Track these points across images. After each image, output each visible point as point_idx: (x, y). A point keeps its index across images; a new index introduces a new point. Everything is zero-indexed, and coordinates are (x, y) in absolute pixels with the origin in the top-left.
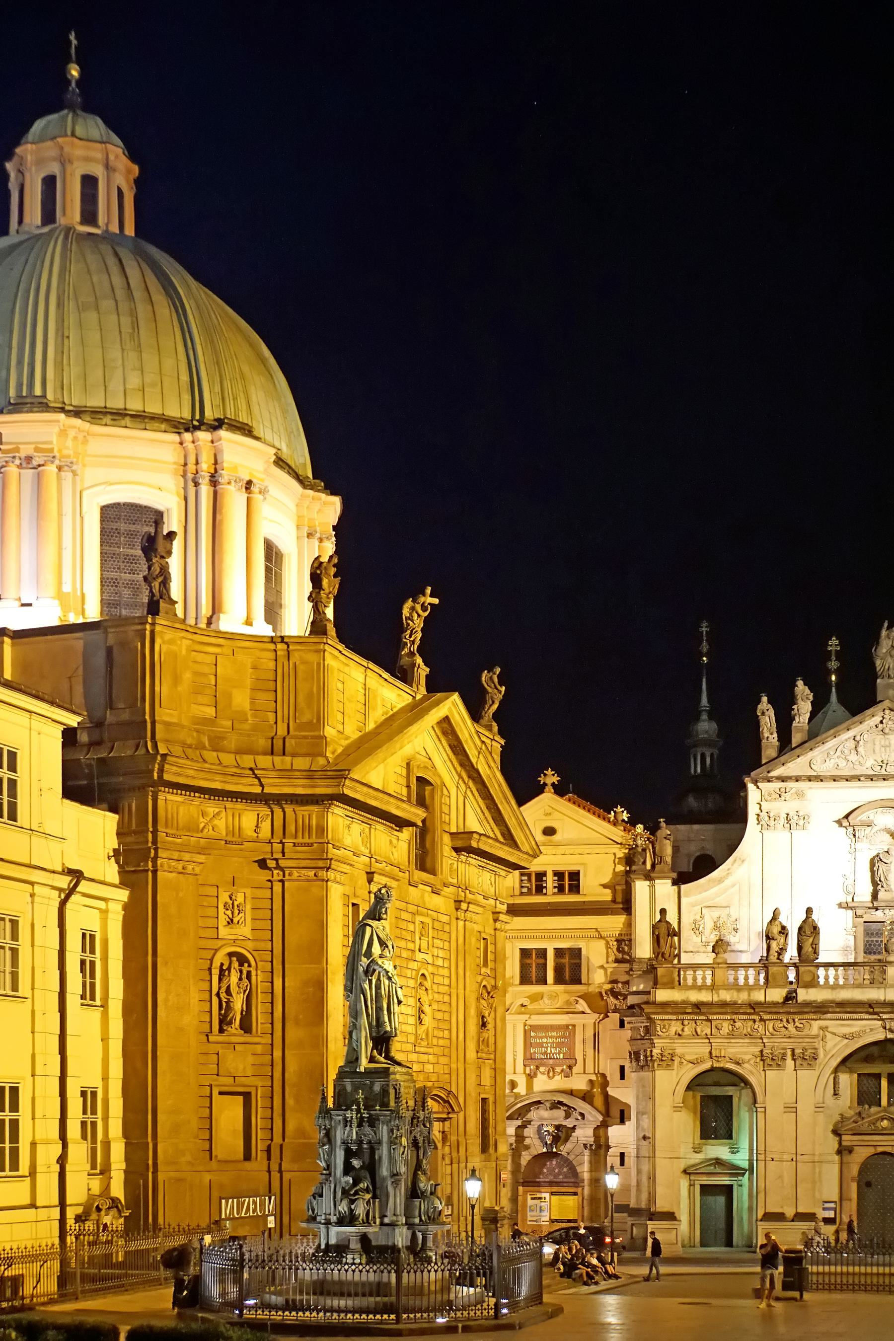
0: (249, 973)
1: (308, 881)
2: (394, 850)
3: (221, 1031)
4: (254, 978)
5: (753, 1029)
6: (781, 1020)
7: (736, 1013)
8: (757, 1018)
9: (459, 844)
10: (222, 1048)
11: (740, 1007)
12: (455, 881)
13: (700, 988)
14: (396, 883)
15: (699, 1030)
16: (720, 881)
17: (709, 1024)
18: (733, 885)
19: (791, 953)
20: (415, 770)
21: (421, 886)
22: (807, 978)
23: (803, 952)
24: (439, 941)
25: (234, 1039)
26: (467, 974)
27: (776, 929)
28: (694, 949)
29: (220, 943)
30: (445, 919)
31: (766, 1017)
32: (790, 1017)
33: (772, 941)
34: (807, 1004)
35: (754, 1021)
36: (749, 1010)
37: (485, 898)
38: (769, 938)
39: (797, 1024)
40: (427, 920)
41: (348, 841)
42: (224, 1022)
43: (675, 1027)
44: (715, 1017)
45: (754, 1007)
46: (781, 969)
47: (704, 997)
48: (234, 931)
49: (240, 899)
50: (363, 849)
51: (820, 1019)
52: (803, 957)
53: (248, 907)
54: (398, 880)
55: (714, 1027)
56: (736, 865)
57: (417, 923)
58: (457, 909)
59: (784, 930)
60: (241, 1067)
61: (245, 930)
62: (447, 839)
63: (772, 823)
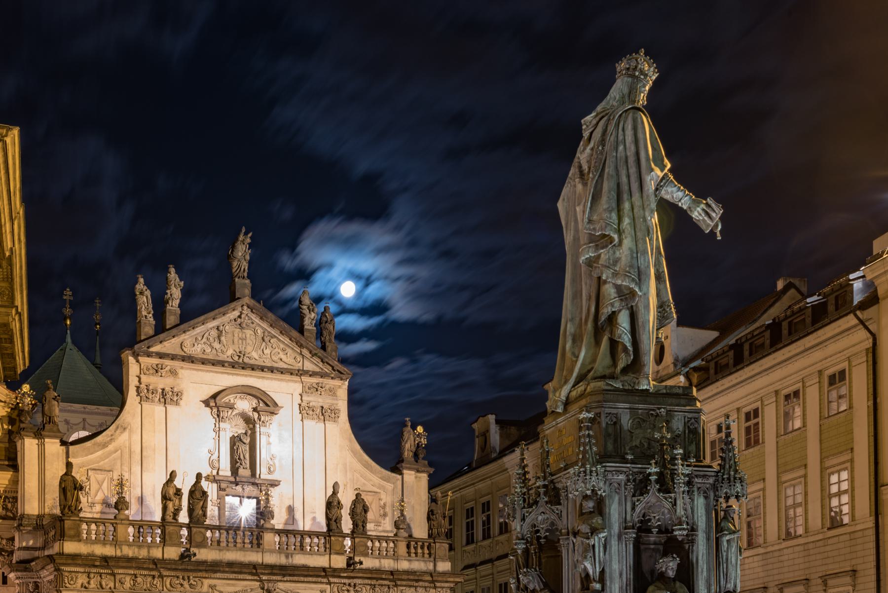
5: (152, 584)
6: (178, 577)
7: (139, 568)
8: (156, 573)
11: (144, 563)
13: (104, 543)
15: (104, 584)
16: (104, 445)
17: (113, 578)
18: (116, 451)
19: (183, 517)
22: (198, 539)
23: (195, 514)
27: (171, 491)
28: (91, 504)
31: (165, 573)
32: (186, 574)
33: (168, 502)
34: (204, 563)
35: (154, 577)
36: (151, 566)
38: (165, 498)
39: (192, 581)
43: (82, 579)
44: (121, 571)
45: (156, 563)
46: (176, 528)
47: (108, 551)
51: (211, 578)
52: (195, 519)
55: (117, 581)
56: (118, 432)
59: (178, 493)
63: (150, 396)
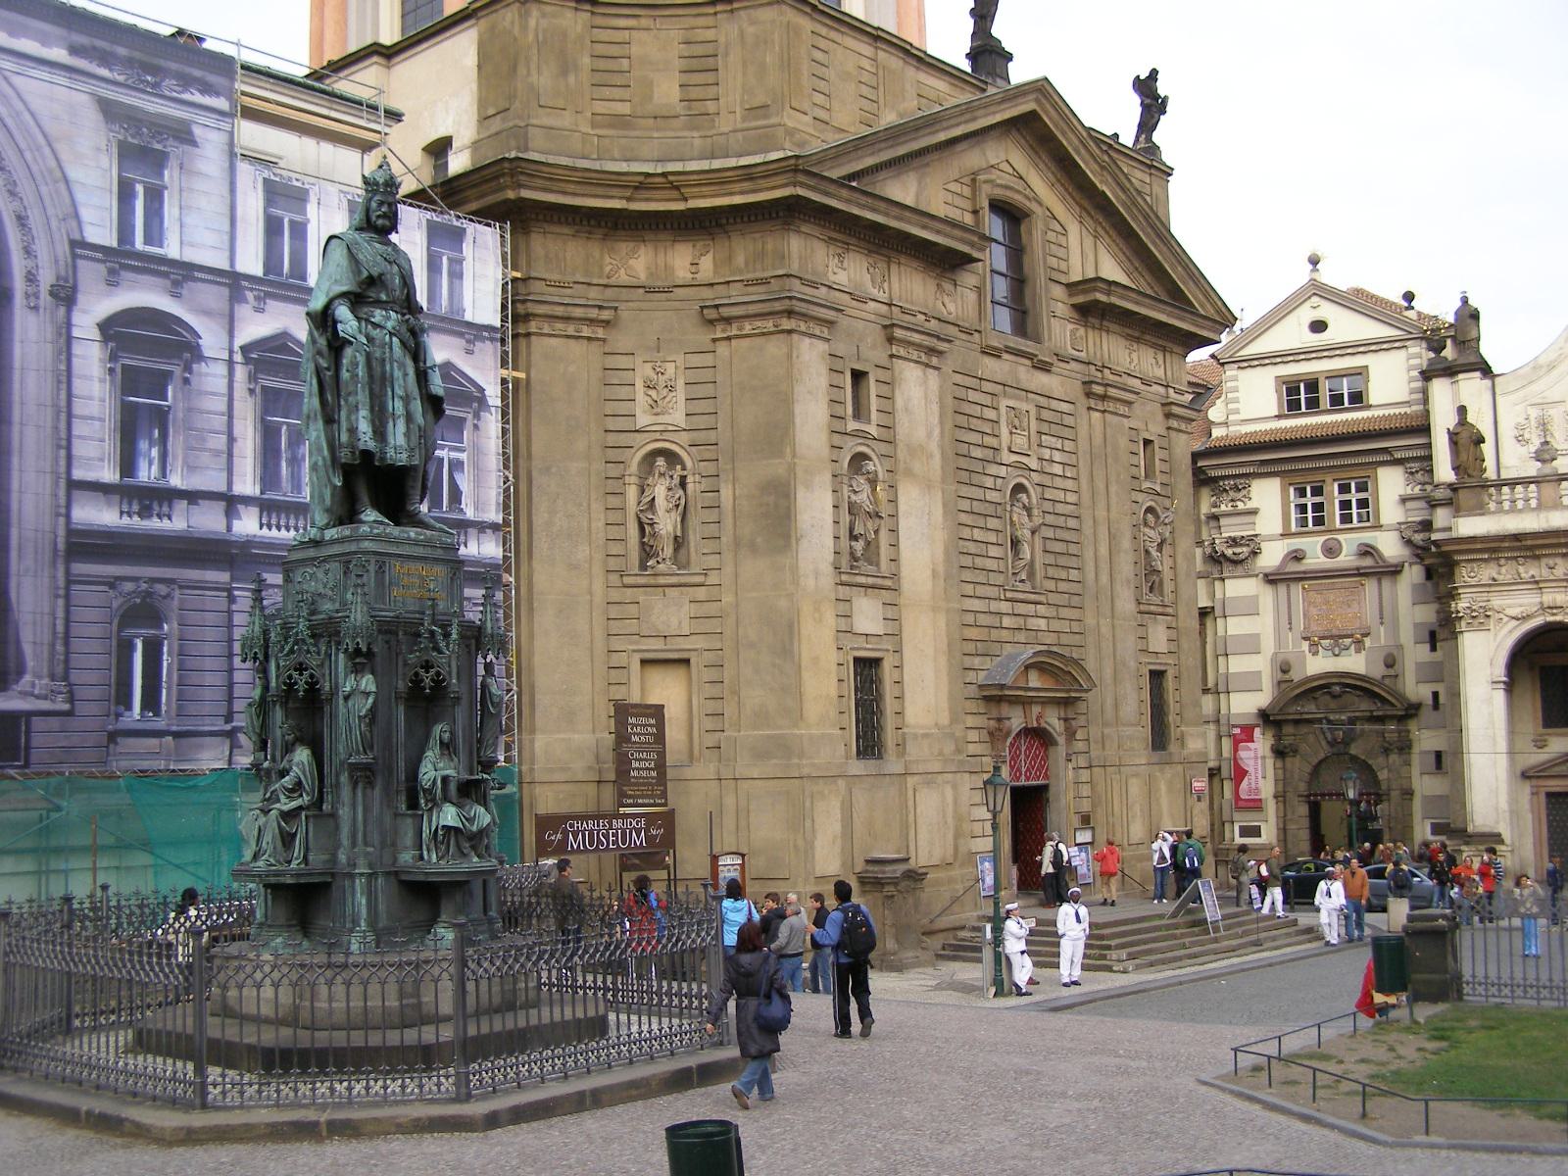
0: (683, 478)
1: (764, 334)
2: (946, 300)
3: (643, 566)
4: (690, 487)
9: (1080, 299)
10: (646, 594)
12: (1083, 355)
14: (946, 345)
20: (986, 189)
21: (1005, 356)
24: (1054, 439)
25: (662, 580)
26: (1113, 489)
29: (639, 438)
30: (1064, 407)
37: (1146, 382)
40: (1024, 406)
41: (841, 278)
42: (647, 552)
48: (661, 419)
49: (670, 369)
50: (875, 292)
53: (680, 383)
54: (950, 341)
57: (1003, 410)
58: (1089, 395)
60: (674, 621)
61: (678, 417)
62: (1058, 291)
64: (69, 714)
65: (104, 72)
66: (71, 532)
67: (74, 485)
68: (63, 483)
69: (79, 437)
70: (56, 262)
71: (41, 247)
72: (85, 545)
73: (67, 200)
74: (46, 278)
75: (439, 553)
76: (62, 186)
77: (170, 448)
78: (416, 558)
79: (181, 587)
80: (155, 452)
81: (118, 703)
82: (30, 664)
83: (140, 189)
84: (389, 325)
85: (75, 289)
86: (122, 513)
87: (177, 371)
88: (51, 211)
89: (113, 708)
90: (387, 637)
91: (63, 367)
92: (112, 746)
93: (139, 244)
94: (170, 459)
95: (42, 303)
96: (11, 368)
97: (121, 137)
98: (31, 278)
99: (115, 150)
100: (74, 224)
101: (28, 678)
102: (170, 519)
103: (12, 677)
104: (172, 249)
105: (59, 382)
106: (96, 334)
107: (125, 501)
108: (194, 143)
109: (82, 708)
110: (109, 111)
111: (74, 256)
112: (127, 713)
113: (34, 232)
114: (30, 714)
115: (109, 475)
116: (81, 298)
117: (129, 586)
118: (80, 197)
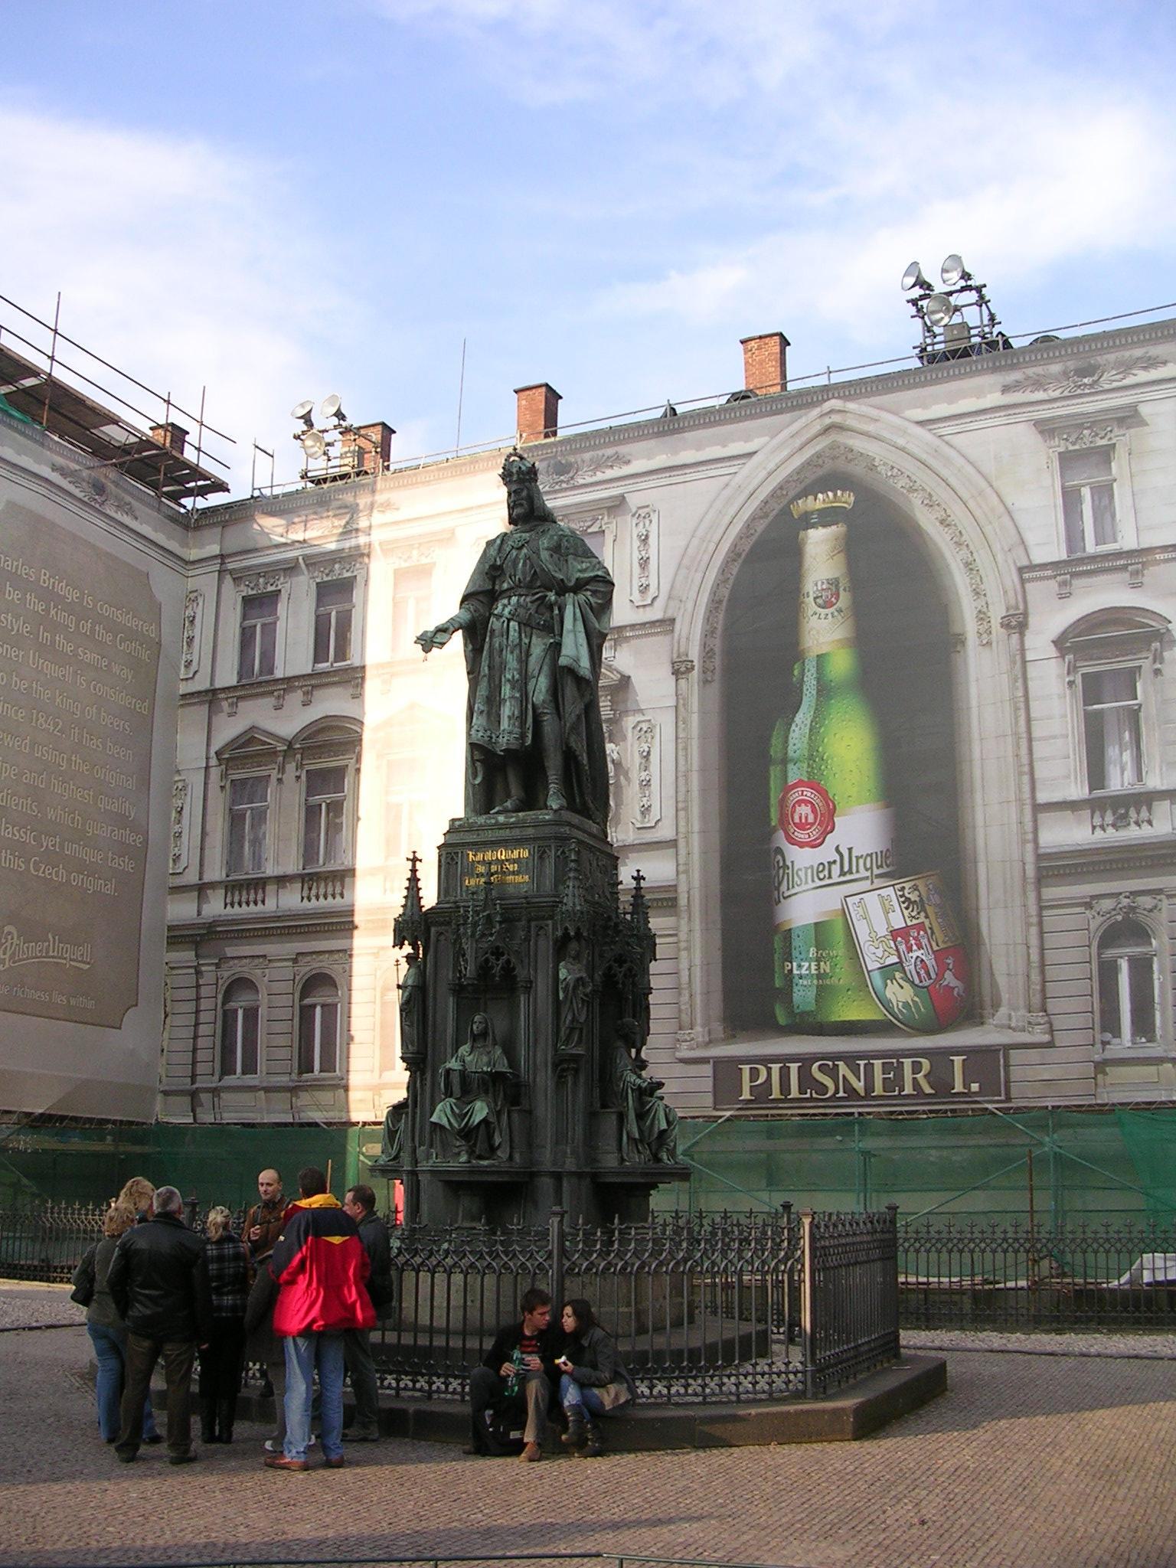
64: (1050, 1045)
65: (1040, 395)
66: (1039, 857)
67: (1038, 808)
68: (1028, 810)
69: (1041, 759)
70: (1005, 592)
71: (991, 585)
72: (1054, 868)
73: (1013, 531)
74: (997, 613)
75: (530, 831)
76: (1006, 519)
77: (1143, 747)
78: (493, 843)
79: (1169, 897)
80: (1127, 757)
81: (1104, 1029)
82: (1005, 997)
83: (1086, 492)
84: (507, 610)
85: (1025, 614)
86: (1094, 828)
87: (1147, 665)
88: (996, 547)
89: (1098, 1037)
90: (441, 929)
91: (1020, 693)
92: (1100, 1077)
93: (1091, 548)
94: (1145, 759)
95: (994, 636)
96: (969, 708)
97: (1061, 450)
98: (982, 616)
99: (1056, 464)
100: (1021, 551)
101: (1003, 1010)
102: (1150, 823)
103: (988, 1010)
104: (1128, 541)
105: (1017, 709)
106: (1052, 652)
107: (1097, 814)
108: (1143, 423)
109: (1061, 1039)
110: (1046, 429)
111: (1023, 581)
112: (1116, 1041)
113: (981, 572)
114: (1008, 1048)
115: (1078, 790)
116: (1032, 620)
117: (1107, 904)
118: (1022, 520)
